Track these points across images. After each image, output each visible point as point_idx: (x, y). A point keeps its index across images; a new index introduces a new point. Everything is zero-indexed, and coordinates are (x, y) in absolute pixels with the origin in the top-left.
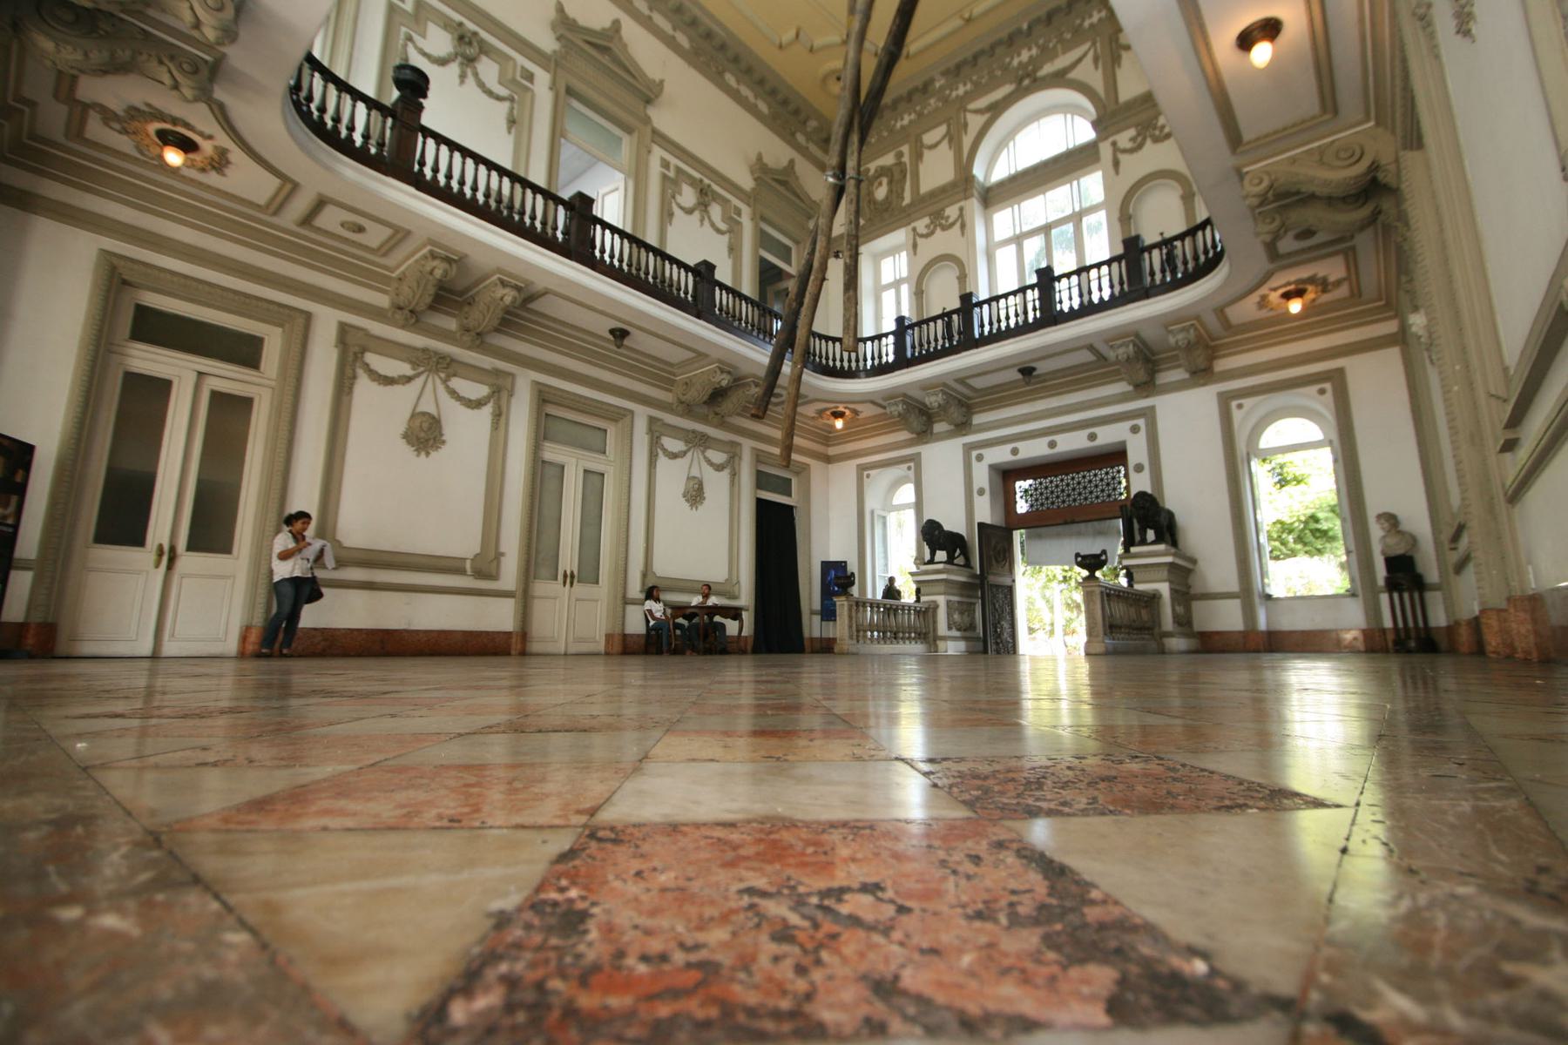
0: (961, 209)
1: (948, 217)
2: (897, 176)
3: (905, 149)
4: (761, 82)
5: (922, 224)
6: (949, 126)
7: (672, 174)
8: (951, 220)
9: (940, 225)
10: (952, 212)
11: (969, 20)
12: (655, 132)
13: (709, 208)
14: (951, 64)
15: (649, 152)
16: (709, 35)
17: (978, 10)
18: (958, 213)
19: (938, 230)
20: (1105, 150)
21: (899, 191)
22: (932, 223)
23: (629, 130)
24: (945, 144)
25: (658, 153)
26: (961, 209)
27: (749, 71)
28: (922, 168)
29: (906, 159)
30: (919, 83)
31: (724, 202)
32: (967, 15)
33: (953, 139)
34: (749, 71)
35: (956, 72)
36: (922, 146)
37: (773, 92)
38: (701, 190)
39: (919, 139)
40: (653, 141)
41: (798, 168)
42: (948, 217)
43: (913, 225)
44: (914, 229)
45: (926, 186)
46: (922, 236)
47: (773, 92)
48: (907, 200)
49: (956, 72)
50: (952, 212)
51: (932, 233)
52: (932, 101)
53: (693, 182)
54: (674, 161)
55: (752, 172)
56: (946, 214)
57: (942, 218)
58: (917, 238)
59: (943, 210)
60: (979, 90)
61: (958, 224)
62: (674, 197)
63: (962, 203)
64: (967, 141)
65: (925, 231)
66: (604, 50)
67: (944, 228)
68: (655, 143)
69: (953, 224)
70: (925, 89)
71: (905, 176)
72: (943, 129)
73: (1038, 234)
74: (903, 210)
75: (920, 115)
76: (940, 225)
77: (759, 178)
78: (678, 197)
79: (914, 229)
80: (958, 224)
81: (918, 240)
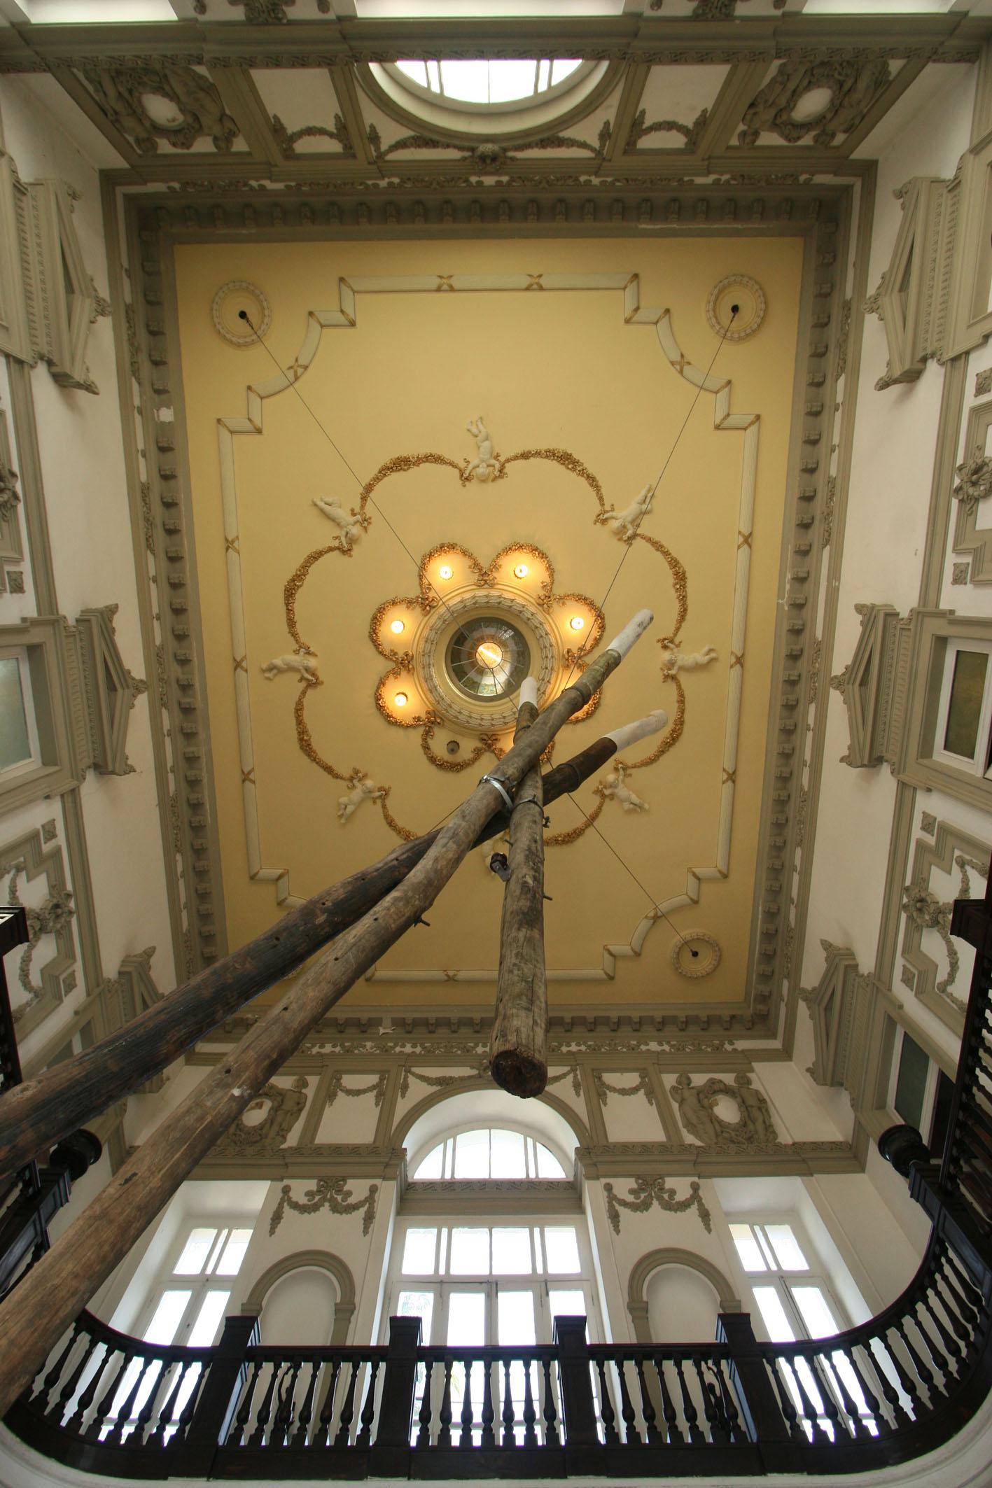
0: (373, 1189)
1: (349, 1194)
2: (289, 1104)
3: (313, 1081)
4: (203, 896)
5: (301, 1188)
6: (381, 1080)
7: (47, 848)
8: (352, 1200)
9: (332, 1200)
10: (357, 1188)
11: (451, 980)
12: (74, 792)
13: (43, 936)
14: (409, 1016)
15: (48, 797)
16: (196, 807)
17: (463, 975)
18: (366, 1194)
19: (325, 1209)
20: (593, 1193)
21: (285, 1125)
22: (319, 1191)
23: (49, 758)
24: (371, 1096)
25: (52, 811)
26: (373, 1189)
27: (201, 874)
28: (328, 1112)
29: (310, 1092)
30: (364, 1016)
31: (66, 954)
32: (451, 973)
33: (385, 1095)
34: (201, 874)
35: (407, 1027)
36: (339, 1085)
37: (205, 917)
38: (57, 906)
39: (337, 1076)
40: (62, 796)
41: (881, 372)
42: (349, 1194)
43: (286, 1182)
44: (286, 1190)
45: (325, 1136)
46: (295, 1206)
47: (205, 917)
48: (292, 1139)
49: (407, 1027)
50: (357, 1188)
51: (315, 1208)
52: (369, 1044)
53: (56, 886)
54: (61, 839)
55: (125, 962)
56: (346, 1188)
57: (339, 1191)
58: (286, 1207)
59: (344, 1179)
60: (428, 1058)
61: (362, 1211)
62: (19, 869)
63: (377, 1182)
64: (402, 1107)
65: (303, 1200)
66: (112, 688)
67: (336, 1209)
68: (63, 803)
69: (355, 1207)
70: (364, 1027)
71: (300, 1110)
72: (373, 1079)
73: (477, 1291)
74: (283, 1154)
75: (348, 1051)
76: (332, 1200)
77: (129, 973)
78: (23, 875)
79: (286, 1190)
80: (362, 1211)
81: (286, 1207)
